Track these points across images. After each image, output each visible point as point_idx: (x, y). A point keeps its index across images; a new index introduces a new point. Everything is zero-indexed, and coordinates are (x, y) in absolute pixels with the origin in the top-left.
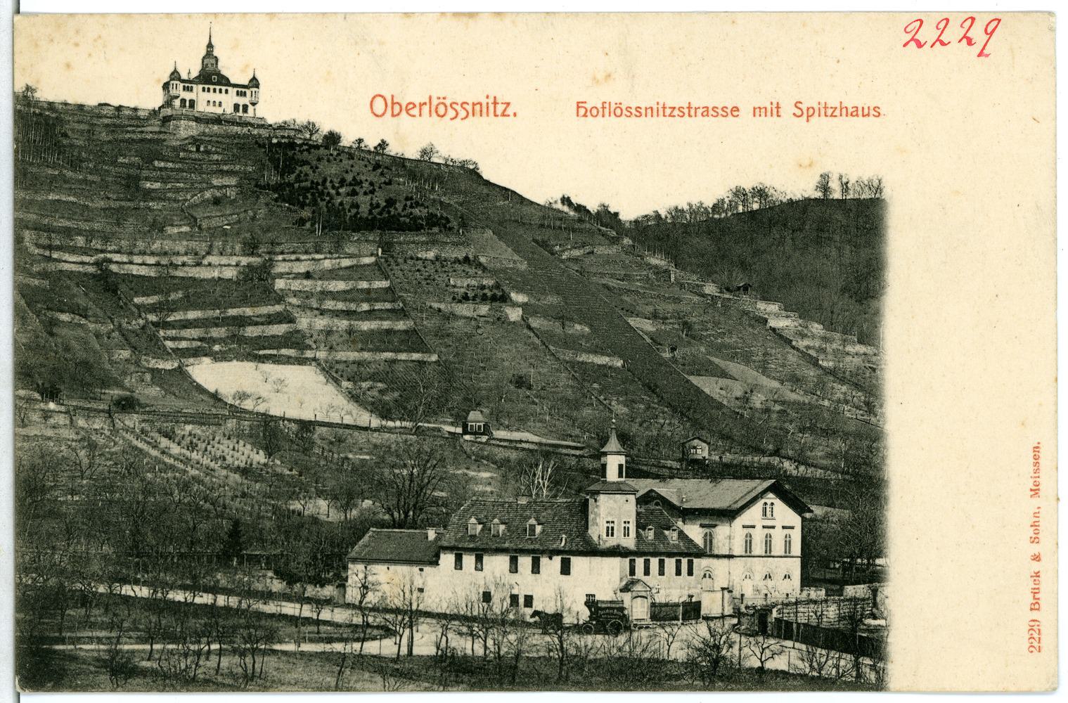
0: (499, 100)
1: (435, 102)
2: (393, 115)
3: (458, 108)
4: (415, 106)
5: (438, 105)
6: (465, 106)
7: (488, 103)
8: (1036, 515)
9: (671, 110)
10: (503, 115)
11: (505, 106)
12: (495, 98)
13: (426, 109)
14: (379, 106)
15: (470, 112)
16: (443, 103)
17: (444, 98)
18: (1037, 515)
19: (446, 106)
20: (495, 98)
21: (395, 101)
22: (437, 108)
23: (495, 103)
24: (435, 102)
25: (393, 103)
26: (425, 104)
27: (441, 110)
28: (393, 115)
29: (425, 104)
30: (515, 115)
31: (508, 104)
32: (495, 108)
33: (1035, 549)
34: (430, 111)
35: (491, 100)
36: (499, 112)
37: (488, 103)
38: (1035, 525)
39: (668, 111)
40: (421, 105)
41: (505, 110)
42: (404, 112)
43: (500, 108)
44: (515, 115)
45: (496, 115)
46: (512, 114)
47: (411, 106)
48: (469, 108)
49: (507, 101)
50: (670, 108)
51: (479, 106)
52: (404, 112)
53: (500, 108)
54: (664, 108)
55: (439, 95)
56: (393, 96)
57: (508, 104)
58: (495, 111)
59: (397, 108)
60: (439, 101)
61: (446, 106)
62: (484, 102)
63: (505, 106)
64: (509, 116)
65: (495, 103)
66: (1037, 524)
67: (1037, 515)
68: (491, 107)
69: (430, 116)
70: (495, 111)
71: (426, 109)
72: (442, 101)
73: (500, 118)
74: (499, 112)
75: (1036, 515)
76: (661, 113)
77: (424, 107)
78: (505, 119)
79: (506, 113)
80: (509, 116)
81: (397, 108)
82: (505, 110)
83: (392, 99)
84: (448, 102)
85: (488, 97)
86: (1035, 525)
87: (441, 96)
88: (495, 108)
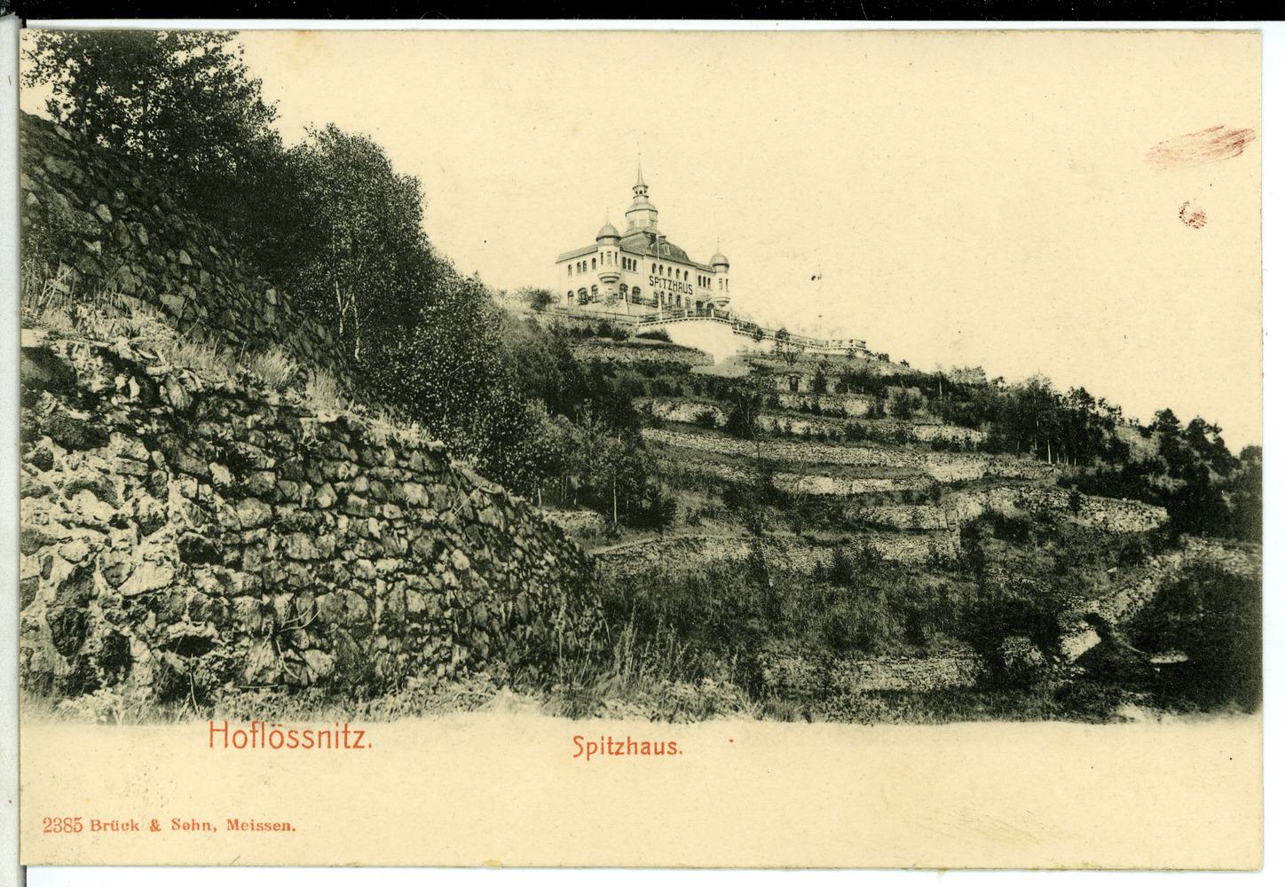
3: (302, 740)
6: (308, 735)
8: (207, 826)
9: (618, 746)
10: (356, 746)
16: (281, 734)
18: (206, 826)
23: (346, 732)
30: (370, 746)
31: (362, 733)
33: (165, 824)
36: (351, 742)
38: (194, 825)
39: (614, 748)
43: (352, 739)
44: (370, 746)
45: (346, 746)
50: (618, 743)
51: (326, 736)
53: (352, 739)
54: (610, 744)
57: (362, 733)
60: (272, 729)
63: (358, 735)
64: (363, 747)
65: (346, 732)
66: (196, 826)
67: (206, 826)
74: (351, 742)
75: (207, 826)
76: (606, 749)
80: (363, 747)
82: (360, 738)
84: (285, 732)
86: (194, 825)
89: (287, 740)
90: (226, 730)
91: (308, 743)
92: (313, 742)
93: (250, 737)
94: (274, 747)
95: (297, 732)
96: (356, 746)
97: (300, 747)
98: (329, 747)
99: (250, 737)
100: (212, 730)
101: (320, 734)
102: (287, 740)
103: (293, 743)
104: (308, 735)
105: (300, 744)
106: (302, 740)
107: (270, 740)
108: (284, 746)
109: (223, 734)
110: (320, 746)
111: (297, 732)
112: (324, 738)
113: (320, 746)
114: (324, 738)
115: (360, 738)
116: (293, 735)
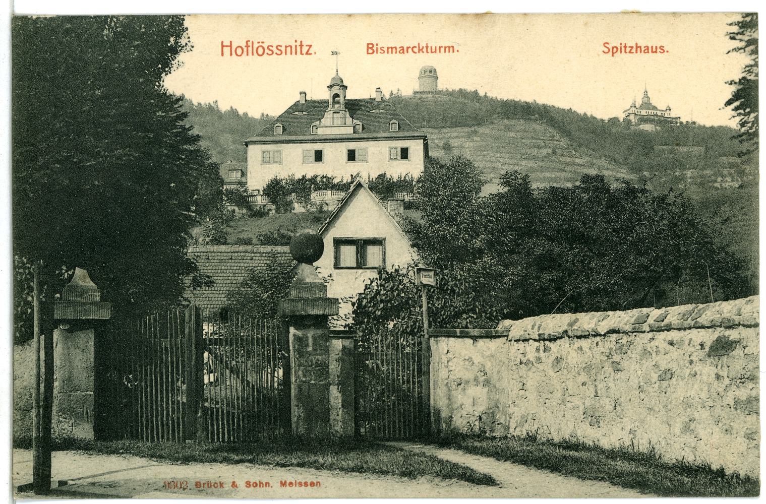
0: (303, 43)
1: (256, 45)
6: (279, 48)
7: (296, 46)
10: (307, 53)
11: (308, 47)
12: (301, 42)
15: (284, 51)
17: (263, 42)
19: (263, 48)
20: (301, 42)
22: (243, 52)
24: (256, 45)
27: (260, 51)
31: (310, 46)
32: (301, 48)
35: (298, 43)
36: (304, 51)
37: (296, 46)
43: (305, 49)
45: (301, 53)
46: (313, 53)
48: (283, 49)
53: (305, 49)
55: (259, 41)
57: (310, 46)
58: (301, 51)
61: (263, 48)
62: (293, 44)
63: (308, 47)
64: (311, 54)
65: (301, 46)
69: (253, 54)
70: (301, 51)
72: (261, 44)
73: (305, 56)
74: (304, 51)
79: (310, 52)
80: (311, 54)
84: (265, 46)
85: (296, 41)
87: (260, 41)
88: (301, 48)
89: (267, 51)
90: (231, 46)
91: (279, 52)
93: (245, 49)
94: (261, 55)
95: (272, 46)
96: (307, 53)
98: (291, 54)
99: (245, 49)
100: (223, 46)
101: (286, 47)
102: (267, 51)
103: (270, 53)
104: (279, 48)
105: (275, 53)
106: (274, 49)
108: (265, 53)
109: (229, 48)
110: (286, 54)
111: (272, 46)
112: (289, 49)
113: (286, 54)
114: (289, 49)
116: (270, 48)
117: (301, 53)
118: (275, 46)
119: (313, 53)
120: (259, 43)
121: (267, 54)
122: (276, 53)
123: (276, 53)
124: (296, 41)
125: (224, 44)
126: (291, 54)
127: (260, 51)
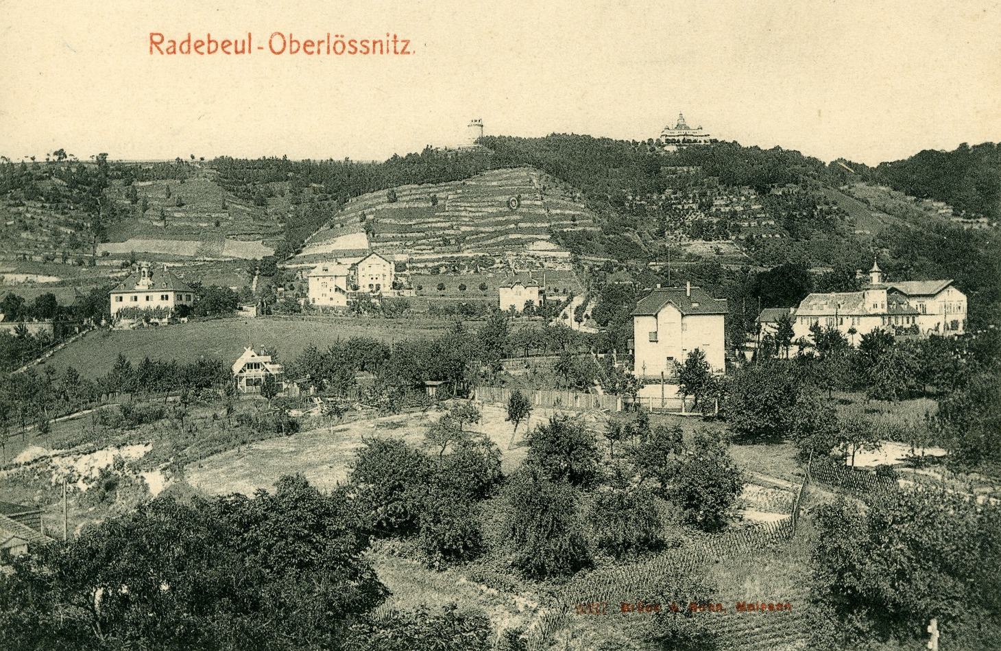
0: (399, 38)
2: (291, 53)
3: (360, 47)
4: (313, 44)
5: (336, 42)
12: (395, 37)
13: (323, 47)
14: (278, 45)
15: (371, 51)
17: (342, 36)
20: (395, 37)
21: (293, 39)
23: (395, 42)
24: (333, 40)
25: (291, 42)
26: (323, 41)
28: (291, 53)
29: (323, 41)
31: (407, 42)
34: (328, 47)
35: (391, 38)
36: (399, 49)
40: (319, 43)
41: (405, 48)
42: (301, 50)
45: (396, 52)
47: (310, 44)
48: (370, 45)
49: (406, 38)
52: (301, 50)
53: (400, 46)
56: (291, 35)
57: (407, 42)
59: (295, 46)
64: (409, 53)
65: (395, 42)
68: (391, 45)
69: (328, 52)
71: (323, 47)
72: (339, 38)
74: (399, 49)
77: (321, 45)
78: (406, 56)
79: (406, 50)
80: (409, 53)
81: (295, 46)
82: (405, 48)
83: (291, 38)
87: (339, 34)
89: (348, 48)
91: (365, 50)
92: (368, 49)
94: (340, 54)
96: (403, 52)
97: (358, 53)
98: (382, 52)
101: (375, 43)
102: (348, 48)
103: (352, 50)
106: (358, 45)
107: (334, 48)
108: (346, 52)
112: (378, 45)
113: (374, 51)
114: (378, 45)
115: (406, 45)
116: (352, 43)
117: (396, 52)
118: (359, 42)
119: (412, 52)
120: (337, 36)
121: (350, 52)
122: (361, 52)
123: (361, 52)
124: (388, 36)
125: (293, 39)
126: (382, 52)
127: (339, 47)
